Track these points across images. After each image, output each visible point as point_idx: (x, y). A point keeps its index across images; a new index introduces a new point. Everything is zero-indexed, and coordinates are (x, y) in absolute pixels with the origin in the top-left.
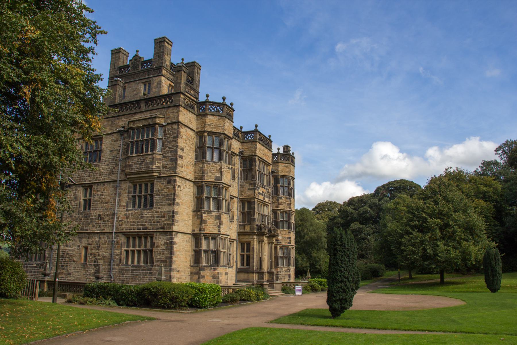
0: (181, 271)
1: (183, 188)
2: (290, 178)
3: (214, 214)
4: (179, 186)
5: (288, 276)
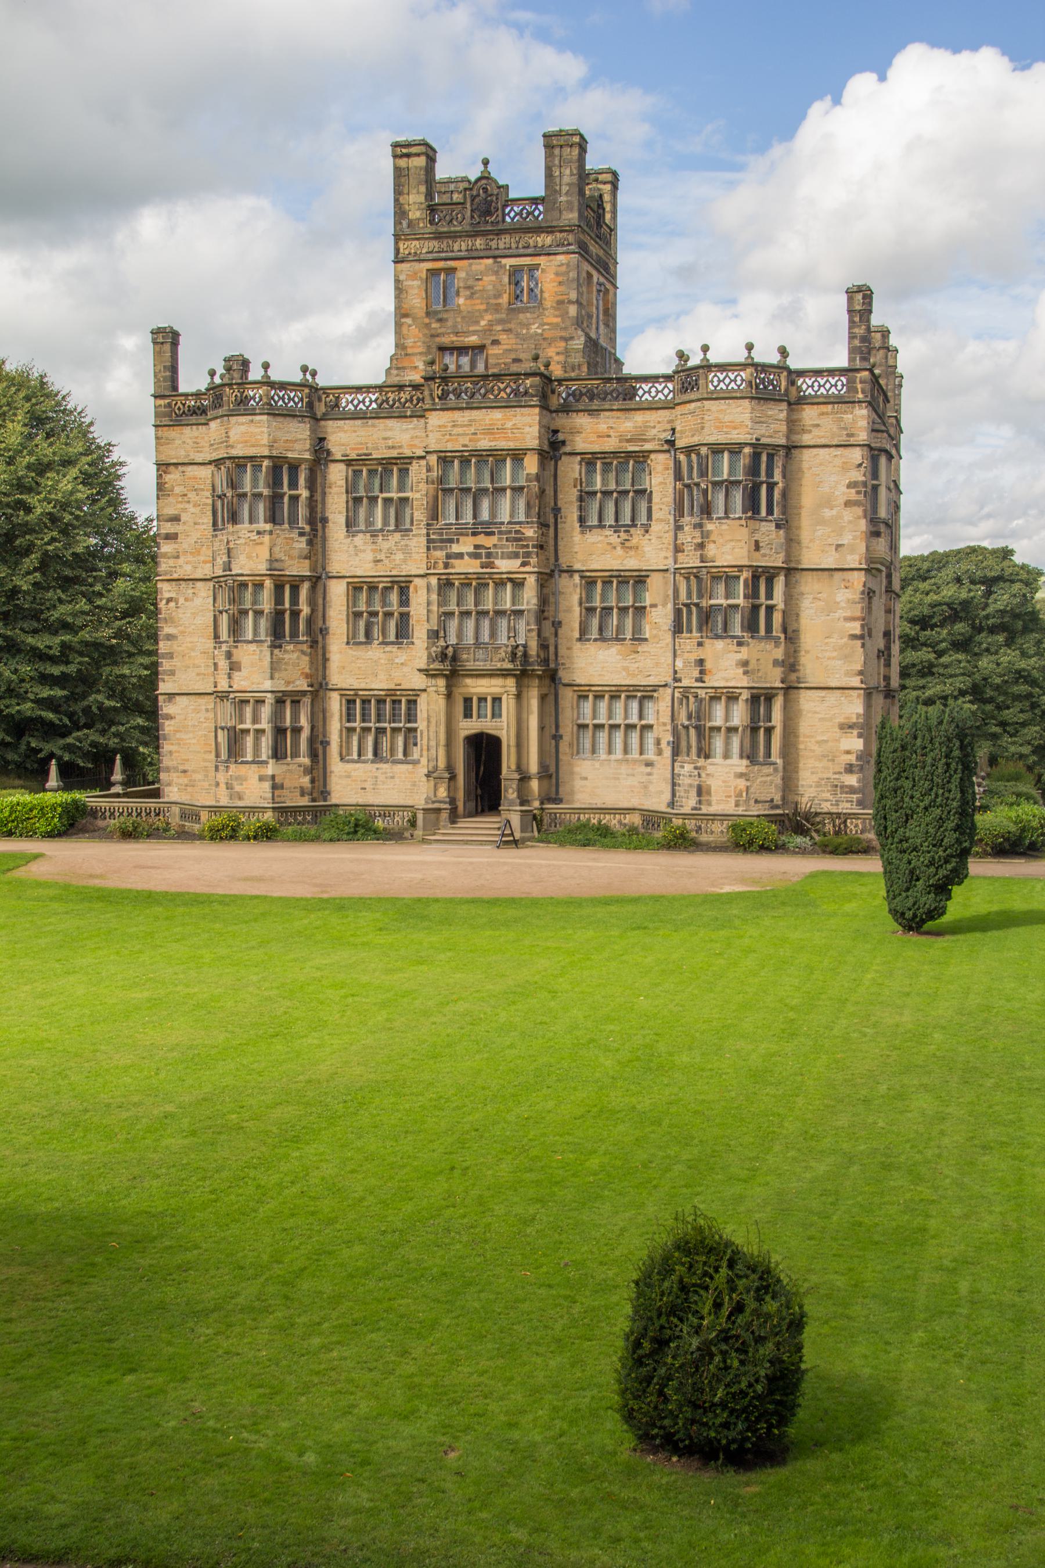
1: (186, 600)
2: (704, 450)
3: (224, 647)
4: (169, 600)
5: (693, 793)
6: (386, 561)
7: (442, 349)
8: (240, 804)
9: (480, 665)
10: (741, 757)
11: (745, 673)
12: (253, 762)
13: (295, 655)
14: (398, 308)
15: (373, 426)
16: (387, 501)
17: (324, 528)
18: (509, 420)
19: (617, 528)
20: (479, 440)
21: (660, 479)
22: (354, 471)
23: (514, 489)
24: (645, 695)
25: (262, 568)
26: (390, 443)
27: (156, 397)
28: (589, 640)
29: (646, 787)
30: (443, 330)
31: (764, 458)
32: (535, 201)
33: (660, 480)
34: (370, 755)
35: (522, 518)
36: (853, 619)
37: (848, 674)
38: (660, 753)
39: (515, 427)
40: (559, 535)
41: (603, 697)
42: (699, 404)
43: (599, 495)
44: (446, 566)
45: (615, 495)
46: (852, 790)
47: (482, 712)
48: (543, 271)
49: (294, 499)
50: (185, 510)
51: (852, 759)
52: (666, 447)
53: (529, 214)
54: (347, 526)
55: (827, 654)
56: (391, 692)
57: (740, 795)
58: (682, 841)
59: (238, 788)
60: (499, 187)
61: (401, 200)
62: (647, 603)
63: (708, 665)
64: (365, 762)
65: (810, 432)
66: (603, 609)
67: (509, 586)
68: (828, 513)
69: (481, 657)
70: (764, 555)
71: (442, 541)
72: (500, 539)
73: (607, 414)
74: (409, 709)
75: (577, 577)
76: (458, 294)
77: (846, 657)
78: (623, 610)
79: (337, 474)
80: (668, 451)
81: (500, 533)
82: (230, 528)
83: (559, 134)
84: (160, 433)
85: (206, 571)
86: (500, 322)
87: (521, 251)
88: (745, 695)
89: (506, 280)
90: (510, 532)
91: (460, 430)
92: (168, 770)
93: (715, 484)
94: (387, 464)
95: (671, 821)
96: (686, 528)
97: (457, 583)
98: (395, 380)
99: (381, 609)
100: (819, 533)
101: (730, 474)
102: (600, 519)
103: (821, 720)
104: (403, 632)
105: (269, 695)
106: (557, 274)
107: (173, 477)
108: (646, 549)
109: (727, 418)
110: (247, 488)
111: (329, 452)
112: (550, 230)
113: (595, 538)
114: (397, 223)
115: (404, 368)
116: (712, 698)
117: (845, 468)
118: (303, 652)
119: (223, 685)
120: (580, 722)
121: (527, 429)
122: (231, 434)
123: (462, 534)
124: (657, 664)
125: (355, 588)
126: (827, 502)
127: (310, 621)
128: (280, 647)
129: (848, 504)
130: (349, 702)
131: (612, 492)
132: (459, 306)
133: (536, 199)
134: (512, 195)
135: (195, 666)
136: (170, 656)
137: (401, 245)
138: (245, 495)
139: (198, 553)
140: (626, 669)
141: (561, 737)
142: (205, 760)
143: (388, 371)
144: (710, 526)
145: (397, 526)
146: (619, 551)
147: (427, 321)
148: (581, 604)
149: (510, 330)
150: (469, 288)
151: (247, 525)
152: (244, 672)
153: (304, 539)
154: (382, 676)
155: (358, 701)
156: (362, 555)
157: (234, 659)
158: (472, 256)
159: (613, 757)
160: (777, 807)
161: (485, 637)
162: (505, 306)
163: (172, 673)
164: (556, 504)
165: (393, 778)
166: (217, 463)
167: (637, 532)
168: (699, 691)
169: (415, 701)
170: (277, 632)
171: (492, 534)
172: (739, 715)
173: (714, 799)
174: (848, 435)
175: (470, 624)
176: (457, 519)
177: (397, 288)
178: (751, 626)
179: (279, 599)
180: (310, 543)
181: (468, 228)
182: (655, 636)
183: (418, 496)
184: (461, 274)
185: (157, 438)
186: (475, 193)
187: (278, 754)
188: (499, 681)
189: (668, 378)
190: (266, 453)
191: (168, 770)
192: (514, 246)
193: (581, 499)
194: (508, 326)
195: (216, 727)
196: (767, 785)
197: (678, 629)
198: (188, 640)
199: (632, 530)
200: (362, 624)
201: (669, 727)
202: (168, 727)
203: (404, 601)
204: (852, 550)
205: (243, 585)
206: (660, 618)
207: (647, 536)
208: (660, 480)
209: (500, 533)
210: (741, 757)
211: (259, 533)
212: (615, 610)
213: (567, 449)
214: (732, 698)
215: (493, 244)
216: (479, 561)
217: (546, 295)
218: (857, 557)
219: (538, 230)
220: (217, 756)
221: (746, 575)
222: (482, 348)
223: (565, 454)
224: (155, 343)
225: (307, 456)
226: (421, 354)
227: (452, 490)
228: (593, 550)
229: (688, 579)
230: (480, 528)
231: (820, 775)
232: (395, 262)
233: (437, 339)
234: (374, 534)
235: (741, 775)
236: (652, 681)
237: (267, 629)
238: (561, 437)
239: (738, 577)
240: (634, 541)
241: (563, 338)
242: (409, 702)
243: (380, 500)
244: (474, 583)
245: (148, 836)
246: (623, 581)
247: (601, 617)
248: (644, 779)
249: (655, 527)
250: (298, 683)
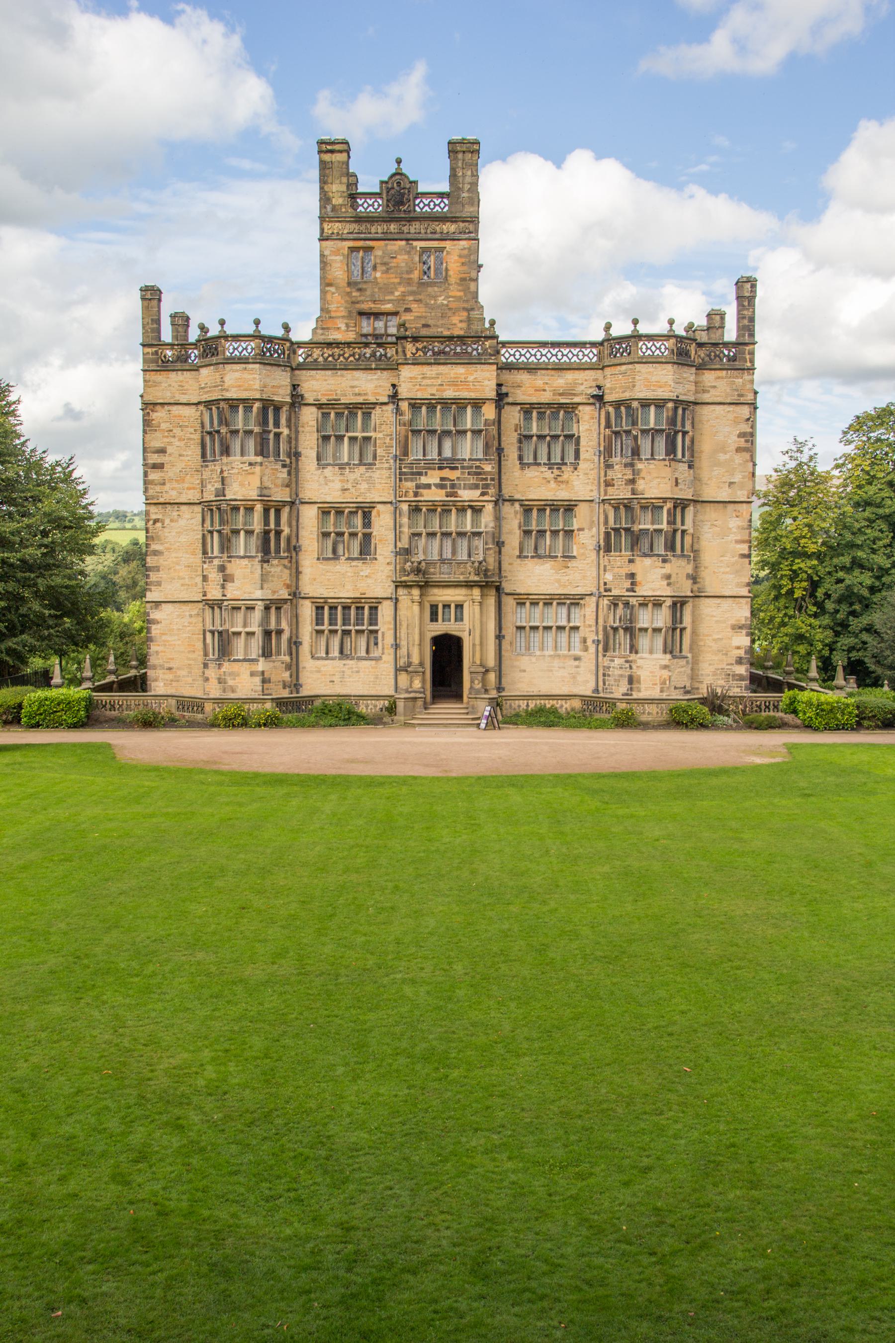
0: (178, 669)
1: (172, 521)
2: (635, 404)
3: (216, 562)
4: (156, 521)
6: (353, 490)
7: (361, 314)
8: (232, 696)
9: (445, 577)
10: (665, 652)
11: (669, 584)
12: (245, 660)
13: (279, 569)
14: (323, 278)
15: (342, 376)
16: (353, 439)
17: (297, 461)
18: (472, 374)
19: (550, 465)
20: (444, 390)
21: (587, 427)
22: (323, 414)
23: (474, 432)
24: (574, 601)
25: (253, 494)
26: (357, 390)
27: (144, 345)
28: (527, 557)
29: (574, 677)
30: (362, 298)
31: (680, 411)
32: (441, 195)
33: (588, 426)
34: (336, 654)
35: (481, 456)
36: (743, 542)
37: (738, 585)
38: (586, 649)
39: (476, 381)
40: (503, 471)
41: (538, 604)
42: (630, 366)
43: (535, 438)
44: (416, 494)
45: (548, 438)
46: (741, 678)
47: (446, 617)
48: (448, 253)
49: (277, 435)
50: (170, 443)
51: (742, 653)
52: (592, 401)
53: (369, 206)
54: (319, 459)
55: (722, 570)
56: (356, 600)
57: (664, 683)
58: (626, 722)
59: (230, 682)
60: (411, 182)
61: (326, 188)
62: (575, 527)
63: (638, 578)
64: (333, 659)
65: (708, 392)
66: (538, 531)
67: (469, 512)
68: (722, 457)
69: (446, 571)
70: (681, 490)
71: (413, 474)
72: (462, 473)
73: (543, 372)
74: (370, 614)
75: (517, 505)
76: (375, 268)
77: (737, 571)
78: (555, 533)
79: (309, 416)
80: (593, 404)
81: (463, 468)
82: (225, 459)
83: (462, 142)
84: (148, 377)
85: (193, 495)
86: (412, 293)
87: (430, 236)
88: (669, 602)
89: (417, 259)
90: (471, 467)
91: (429, 382)
92: (154, 667)
93: (644, 432)
94: (353, 408)
95: (615, 704)
96: (616, 467)
97: (424, 509)
98: (320, 338)
99: (349, 528)
100: (716, 473)
101: (656, 424)
102: (535, 458)
103: (717, 622)
104: (366, 550)
105: (260, 603)
106: (460, 256)
107: (159, 415)
108: (575, 483)
109: (654, 379)
110: (240, 426)
111: (302, 396)
112: (453, 220)
113: (532, 473)
114: (322, 207)
115: (328, 329)
116: (640, 605)
117: (736, 421)
118: (285, 566)
119: (215, 593)
120: (519, 624)
121: (486, 383)
122: (226, 379)
123: (430, 468)
124: (584, 577)
125: (323, 512)
126: (723, 449)
127: (289, 539)
128: (268, 561)
129: (739, 450)
130: (317, 608)
131: (545, 436)
132: (376, 278)
133: (443, 194)
134: (421, 188)
135: (180, 578)
136: (157, 569)
137: (325, 226)
138: (237, 432)
139: (183, 481)
140: (558, 581)
141: (504, 637)
142: (189, 659)
143: (314, 331)
144: (639, 466)
145: (360, 460)
146: (553, 485)
147: (348, 290)
148: (520, 527)
149: (420, 301)
150: (385, 264)
151: (238, 458)
152: (237, 583)
153: (285, 470)
154: (349, 586)
155: (326, 608)
156: (331, 485)
157: (228, 572)
158: (387, 238)
159: (546, 653)
160: (688, 692)
161: (447, 554)
162: (416, 280)
163: (159, 584)
164: (500, 444)
165: (358, 672)
166: (208, 404)
167: (567, 469)
168: (631, 599)
169: (376, 608)
170: (265, 549)
171: (456, 468)
172: (662, 618)
173: (643, 686)
174: (739, 395)
175: (436, 542)
176: (424, 455)
177: (322, 262)
178: (671, 546)
179: (266, 522)
180: (289, 473)
181: (384, 215)
182: (583, 554)
183: (380, 435)
184: (379, 253)
185: (145, 381)
186: (390, 186)
187: (266, 653)
188: (463, 591)
189: (593, 344)
190: (258, 396)
191: (154, 667)
192: (423, 231)
193: (520, 441)
194: (418, 297)
195: (204, 631)
196: (680, 675)
197: (607, 546)
198: (174, 555)
199: (564, 468)
200: (330, 543)
201: (594, 628)
202: (155, 630)
203: (367, 523)
204: (742, 486)
205: (236, 509)
206: (587, 539)
207: (576, 473)
208: (588, 426)
209: (463, 468)
210: (665, 652)
211: (250, 464)
212: (548, 533)
213: (510, 400)
214: (658, 605)
215: (405, 229)
216: (444, 491)
217: (451, 273)
218: (745, 493)
219: (443, 219)
220: (206, 654)
221: (669, 505)
222: (396, 314)
223: (508, 404)
224: (143, 299)
225: (288, 399)
226: (343, 317)
227: (420, 431)
228: (533, 484)
229: (616, 509)
230: (445, 464)
231: (716, 666)
232: (320, 240)
233: (357, 306)
234: (342, 467)
235: (666, 667)
236: (580, 591)
237: (257, 547)
238: (504, 390)
239: (662, 507)
240: (565, 476)
241: (464, 309)
242: (371, 608)
243: (346, 439)
244: (439, 509)
245: (165, 726)
246: (555, 509)
247: (536, 538)
248: (573, 670)
249: (582, 465)
250: (281, 592)
